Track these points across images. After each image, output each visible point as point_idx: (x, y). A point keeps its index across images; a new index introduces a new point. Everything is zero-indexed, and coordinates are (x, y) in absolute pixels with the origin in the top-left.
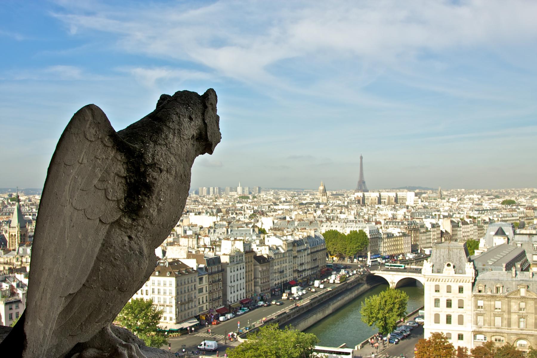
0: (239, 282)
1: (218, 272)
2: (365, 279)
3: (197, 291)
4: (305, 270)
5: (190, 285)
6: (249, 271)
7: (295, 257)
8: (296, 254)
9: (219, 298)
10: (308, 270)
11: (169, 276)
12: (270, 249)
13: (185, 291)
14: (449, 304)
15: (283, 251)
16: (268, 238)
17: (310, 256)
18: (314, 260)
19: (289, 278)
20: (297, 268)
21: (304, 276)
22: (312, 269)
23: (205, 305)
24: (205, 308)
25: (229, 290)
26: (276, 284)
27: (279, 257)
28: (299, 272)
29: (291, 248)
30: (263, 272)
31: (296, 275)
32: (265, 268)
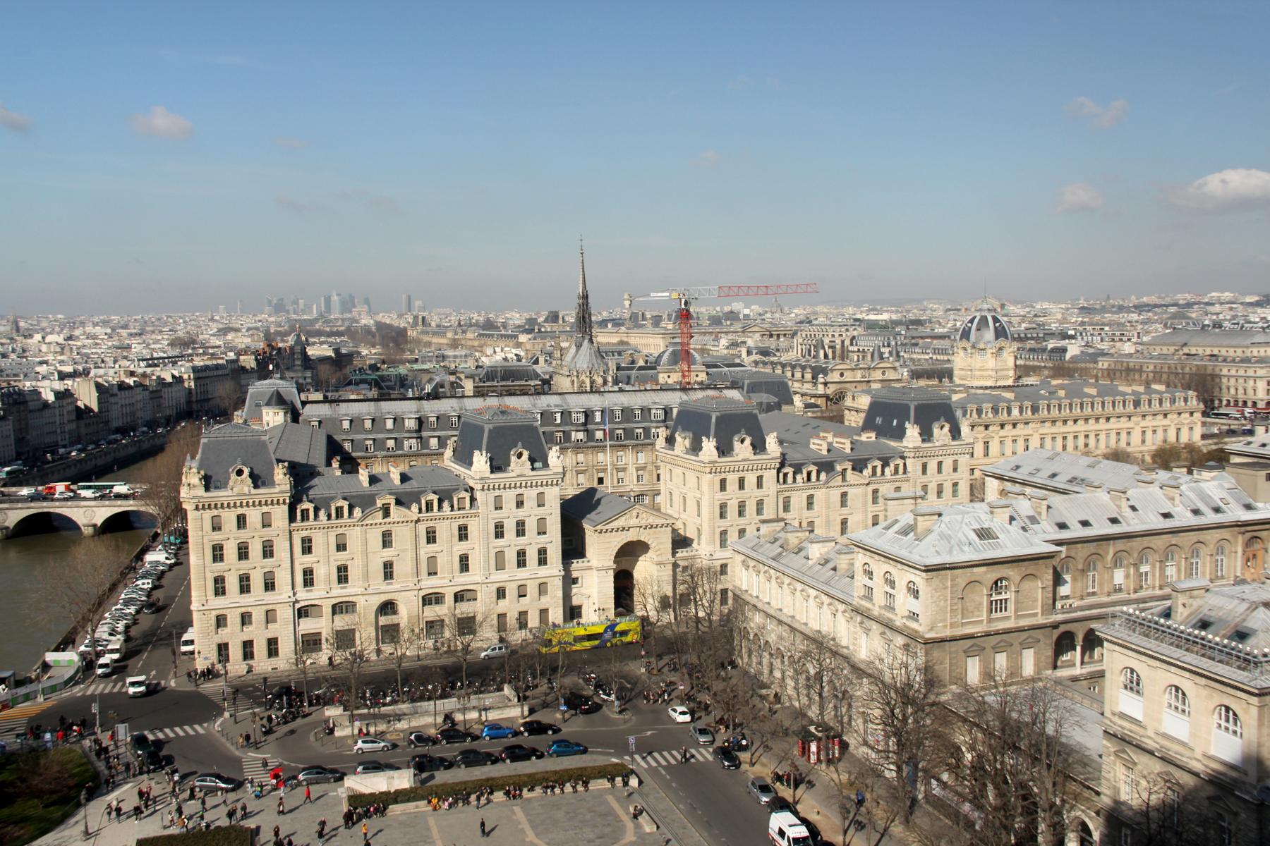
14: (243, 553)
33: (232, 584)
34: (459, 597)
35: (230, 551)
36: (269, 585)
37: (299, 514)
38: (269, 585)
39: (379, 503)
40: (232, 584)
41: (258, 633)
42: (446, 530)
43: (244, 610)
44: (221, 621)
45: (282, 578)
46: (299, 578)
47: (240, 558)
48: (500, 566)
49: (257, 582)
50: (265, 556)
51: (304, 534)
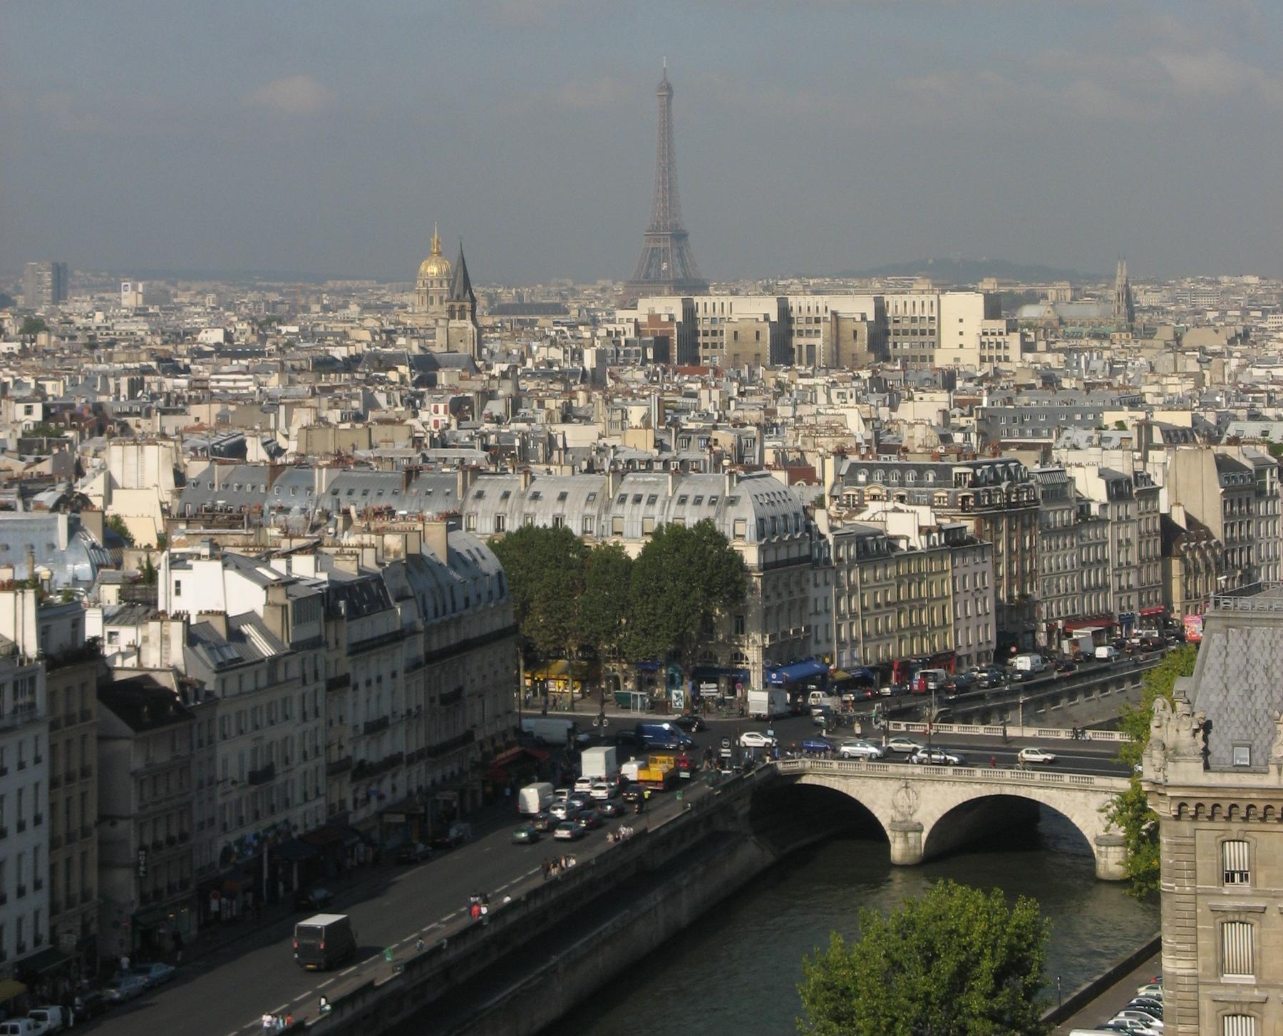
2: (743, 808)
4: (393, 762)
6: (69, 778)
7: (338, 684)
8: (346, 667)
10: (411, 760)
12: (192, 638)
15: (266, 650)
16: (177, 575)
17: (420, 675)
18: (446, 700)
20: (348, 750)
21: (389, 799)
22: (435, 752)
26: (227, 852)
27: (249, 684)
28: (363, 771)
29: (312, 630)
31: (345, 791)
32: (162, 756)
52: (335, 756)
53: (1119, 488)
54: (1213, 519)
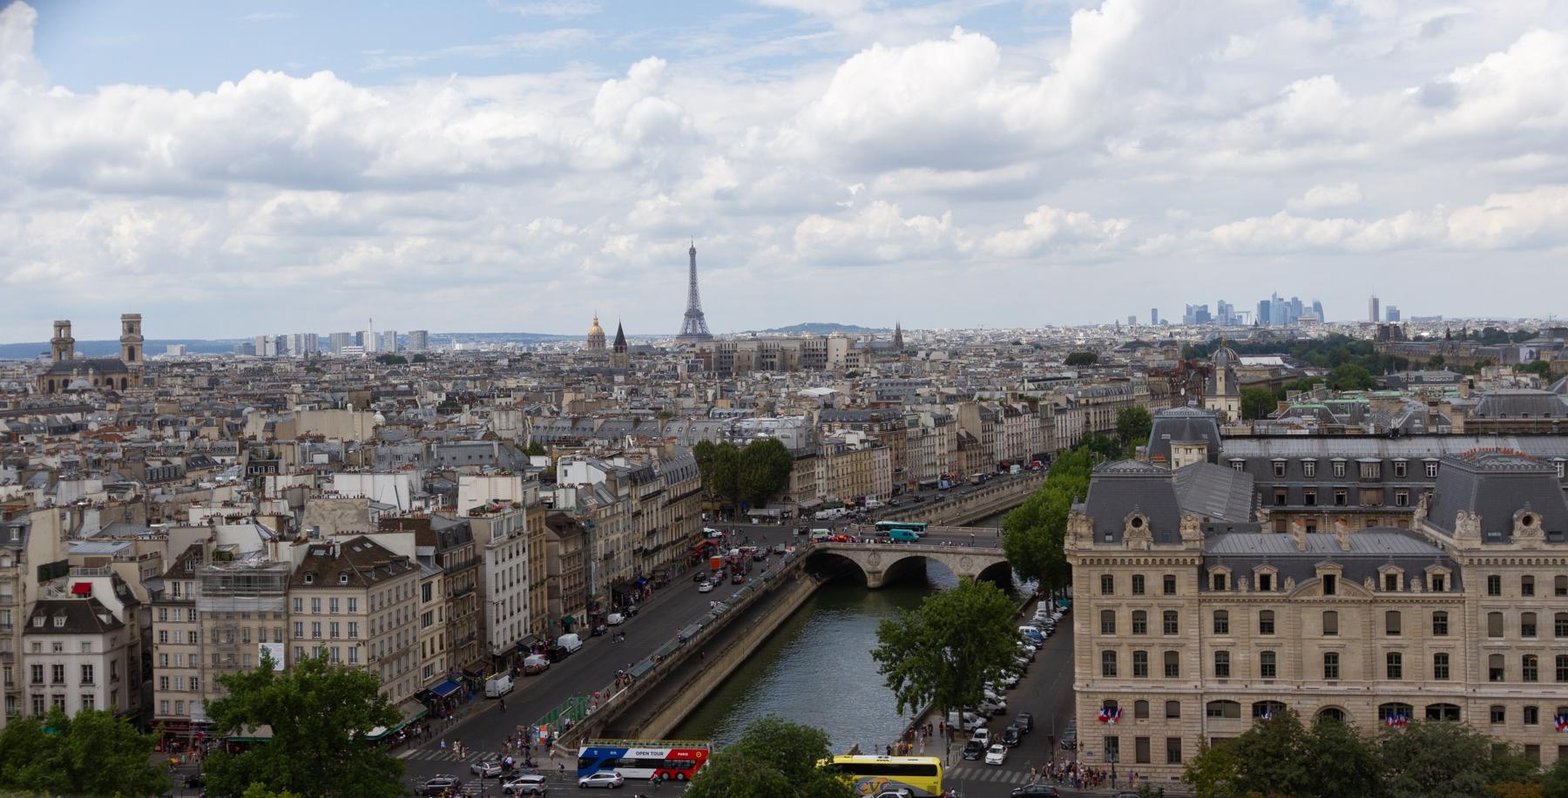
0: (516, 589)
1: (468, 564)
3: (419, 623)
4: (658, 548)
5: (402, 606)
7: (637, 514)
9: (470, 638)
11: (347, 586)
13: (390, 624)
19: (626, 571)
23: (437, 661)
24: (437, 669)
25: (492, 613)
28: (647, 554)
30: (567, 558)
32: (571, 549)
33: (1125, 662)
34: (1432, 712)
35: (1124, 620)
36: (1172, 669)
37: (1212, 580)
38: (1172, 669)
39: (1320, 574)
40: (1125, 662)
41: (1158, 730)
42: (1416, 619)
43: (1138, 697)
44: (1111, 708)
45: (1187, 660)
46: (1210, 664)
47: (1135, 631)
48: (1496, 674)
49: (1156, 662)
50: (1167, 631)
51: (1219, 606)
52: (636, 546)
53: (940, 421)
54: (979, 435)
